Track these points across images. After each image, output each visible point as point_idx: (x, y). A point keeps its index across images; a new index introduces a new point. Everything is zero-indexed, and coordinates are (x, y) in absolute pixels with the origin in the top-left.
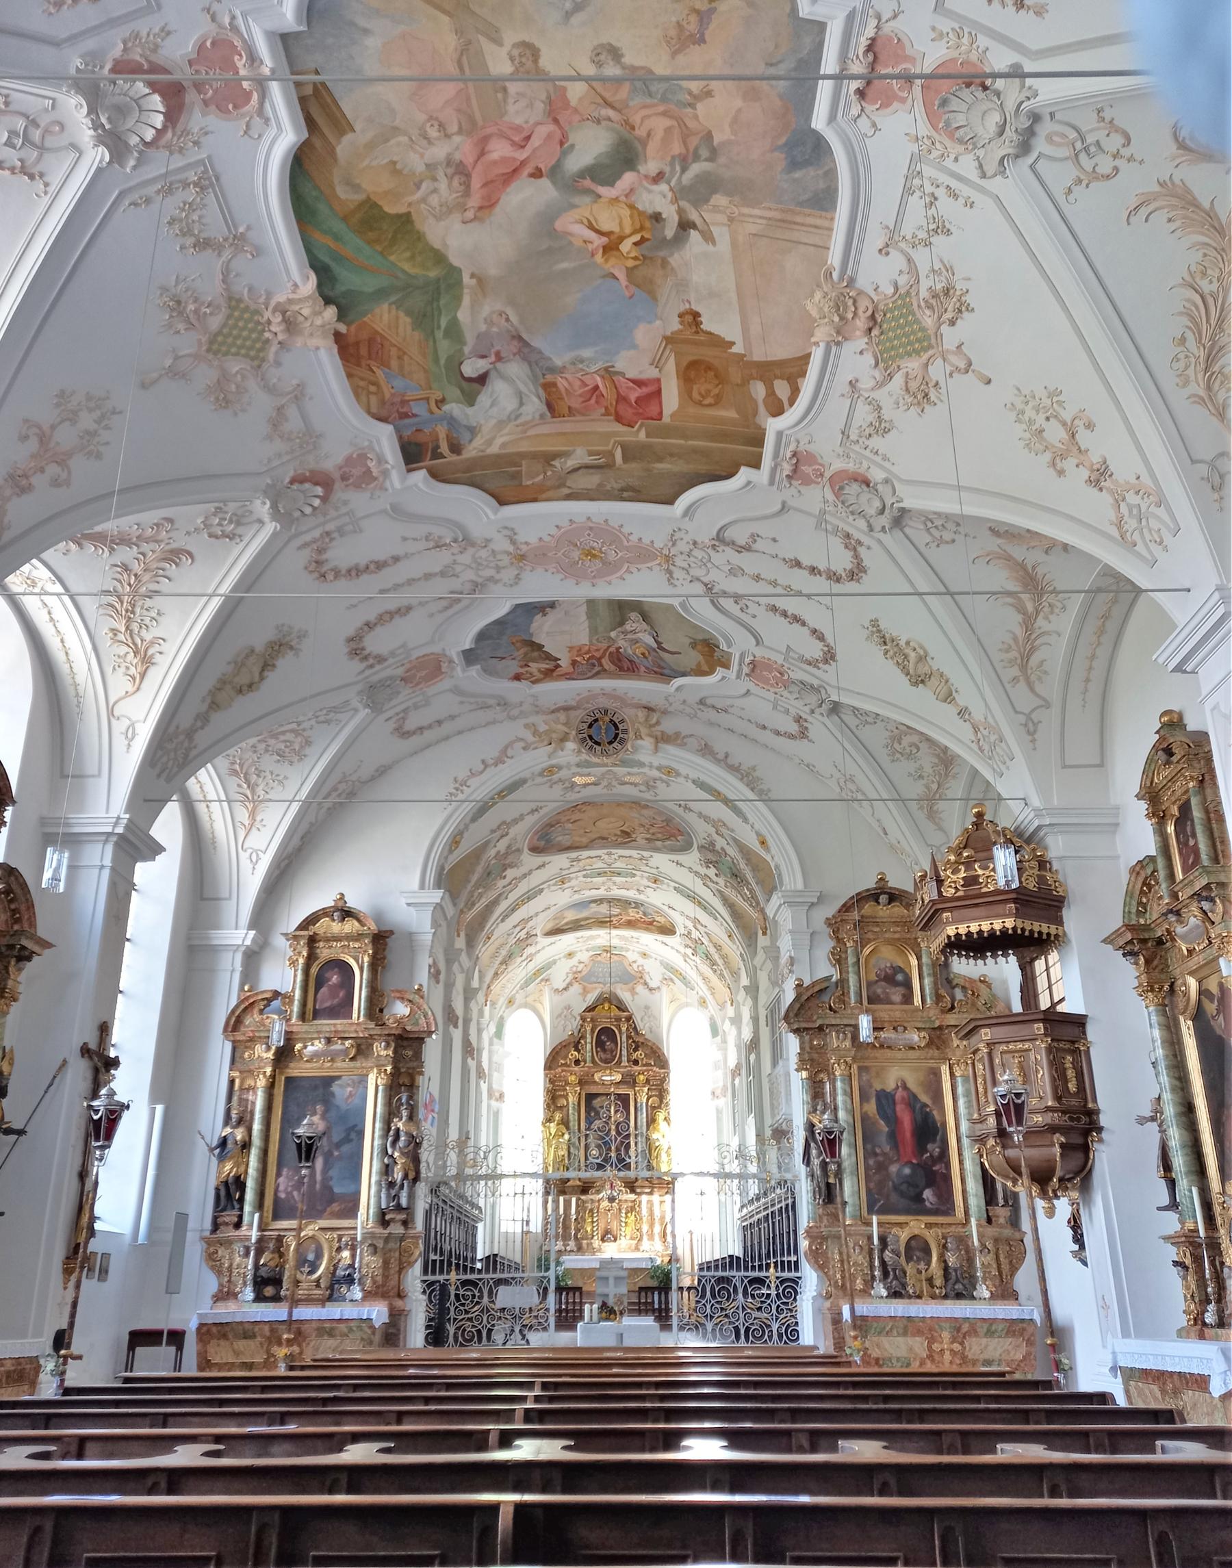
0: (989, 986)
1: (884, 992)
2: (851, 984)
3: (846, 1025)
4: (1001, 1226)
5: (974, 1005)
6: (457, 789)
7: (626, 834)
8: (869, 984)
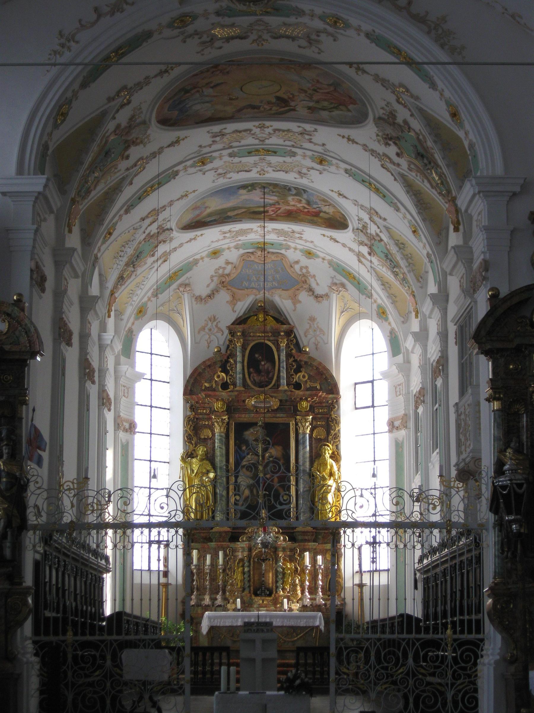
6: (63, 46)
7: (282, 101)
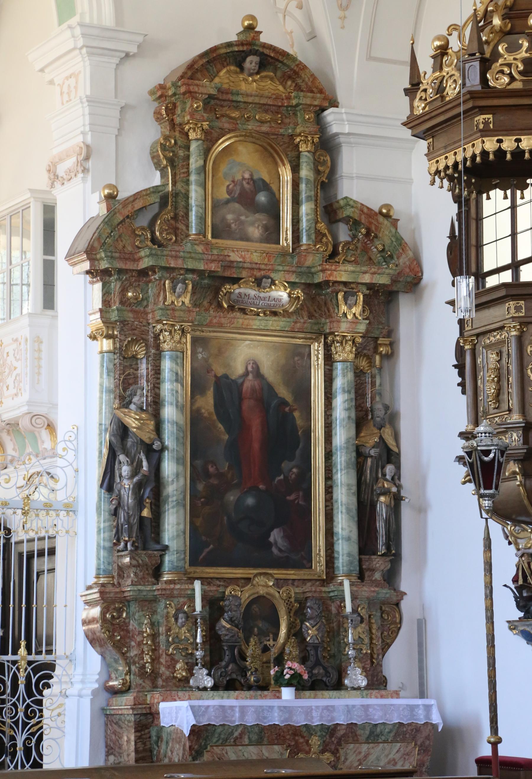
0: (395, 223)
1: (237, 220)
2: (193, 202)
3: (188, 271)
4: (377, 584)
5: (366, 250)
8: (216, 206)
